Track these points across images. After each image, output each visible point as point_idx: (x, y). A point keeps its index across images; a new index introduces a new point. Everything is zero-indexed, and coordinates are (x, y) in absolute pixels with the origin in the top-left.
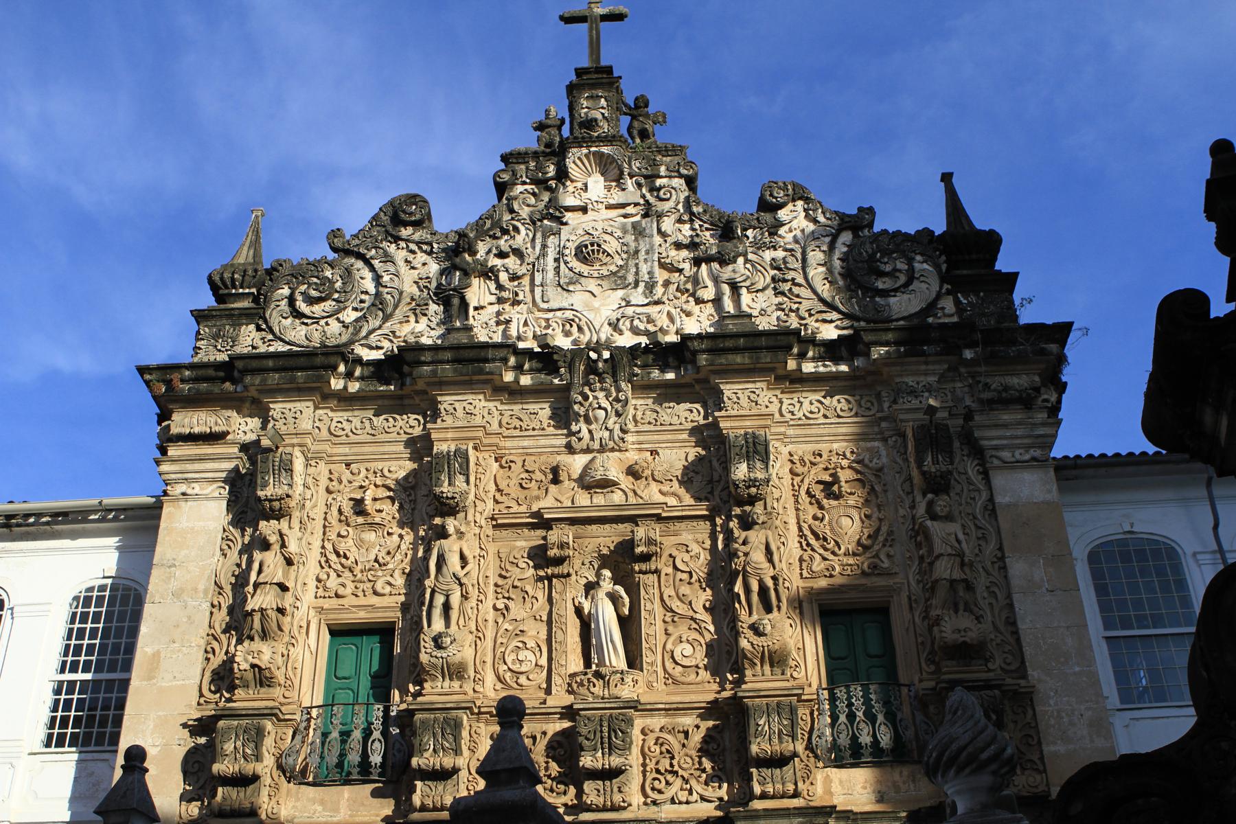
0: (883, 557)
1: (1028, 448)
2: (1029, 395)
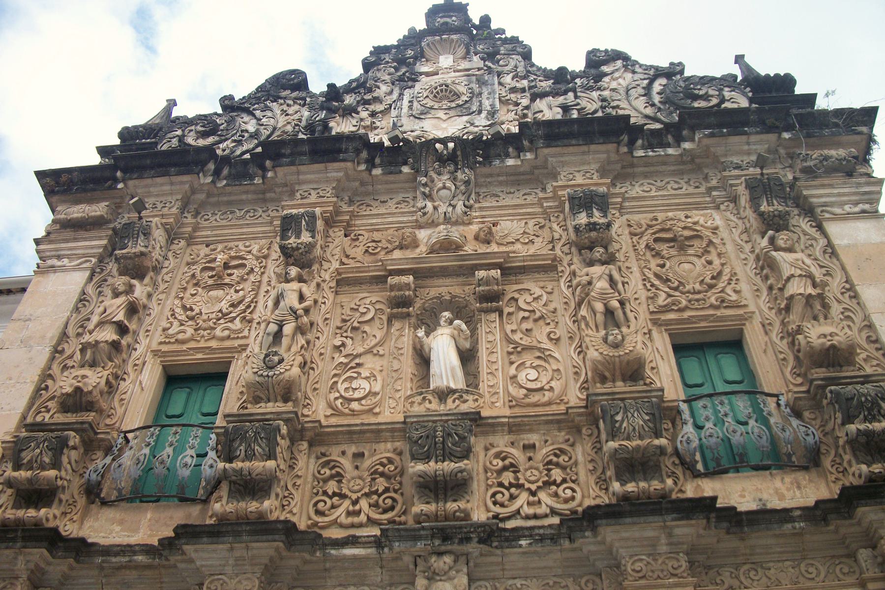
0: (729, 290)
1: (856, 204)
2: (848, 161)
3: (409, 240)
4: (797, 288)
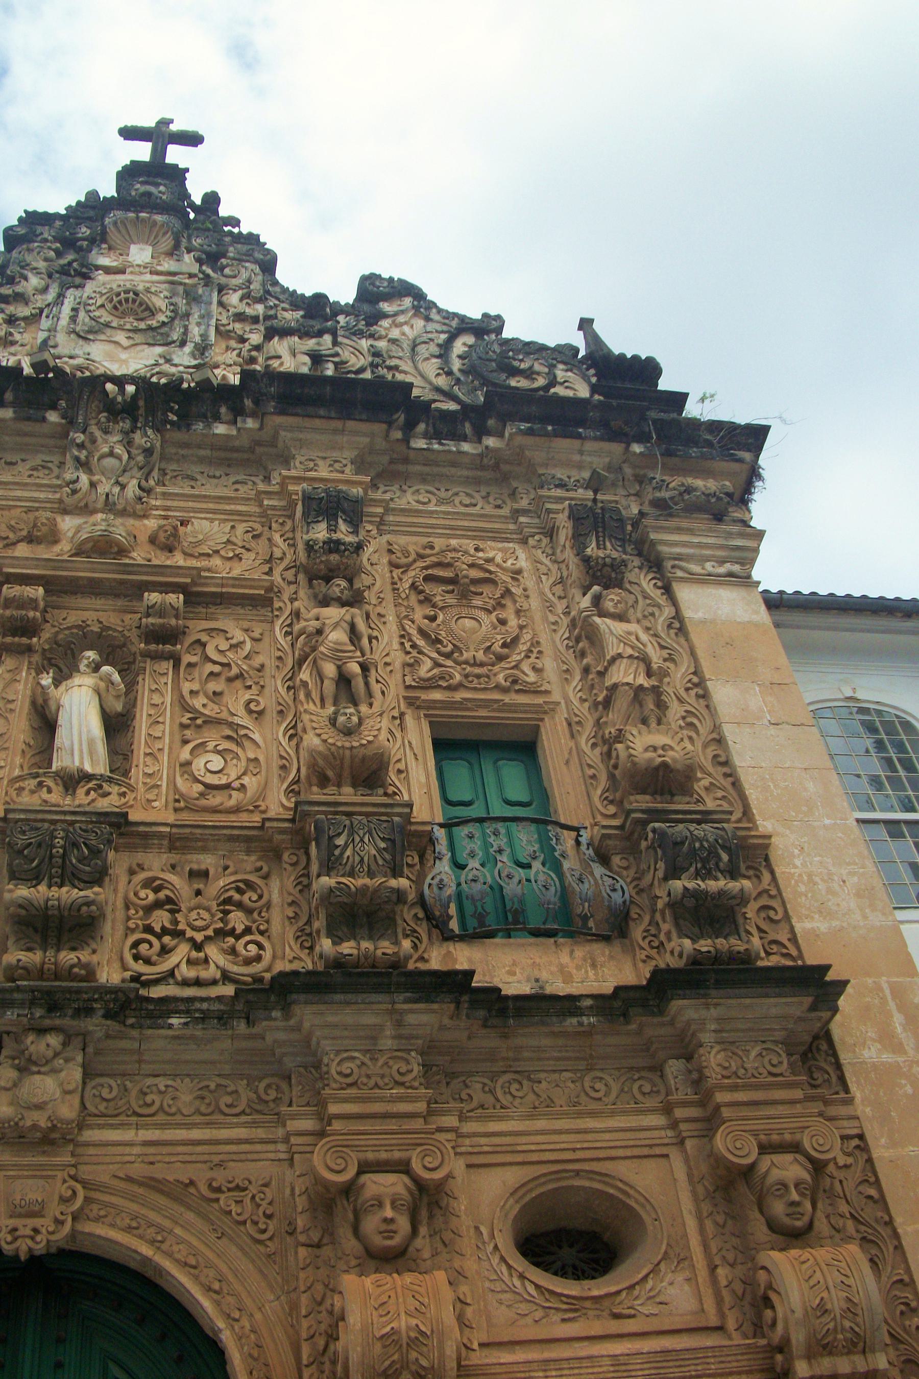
0: (525, 667)
1: (722, 562)
3: (44, 529)
4: (625, 674)
